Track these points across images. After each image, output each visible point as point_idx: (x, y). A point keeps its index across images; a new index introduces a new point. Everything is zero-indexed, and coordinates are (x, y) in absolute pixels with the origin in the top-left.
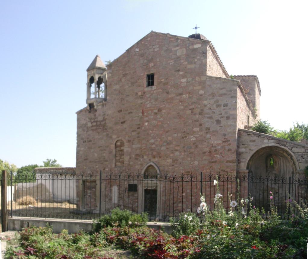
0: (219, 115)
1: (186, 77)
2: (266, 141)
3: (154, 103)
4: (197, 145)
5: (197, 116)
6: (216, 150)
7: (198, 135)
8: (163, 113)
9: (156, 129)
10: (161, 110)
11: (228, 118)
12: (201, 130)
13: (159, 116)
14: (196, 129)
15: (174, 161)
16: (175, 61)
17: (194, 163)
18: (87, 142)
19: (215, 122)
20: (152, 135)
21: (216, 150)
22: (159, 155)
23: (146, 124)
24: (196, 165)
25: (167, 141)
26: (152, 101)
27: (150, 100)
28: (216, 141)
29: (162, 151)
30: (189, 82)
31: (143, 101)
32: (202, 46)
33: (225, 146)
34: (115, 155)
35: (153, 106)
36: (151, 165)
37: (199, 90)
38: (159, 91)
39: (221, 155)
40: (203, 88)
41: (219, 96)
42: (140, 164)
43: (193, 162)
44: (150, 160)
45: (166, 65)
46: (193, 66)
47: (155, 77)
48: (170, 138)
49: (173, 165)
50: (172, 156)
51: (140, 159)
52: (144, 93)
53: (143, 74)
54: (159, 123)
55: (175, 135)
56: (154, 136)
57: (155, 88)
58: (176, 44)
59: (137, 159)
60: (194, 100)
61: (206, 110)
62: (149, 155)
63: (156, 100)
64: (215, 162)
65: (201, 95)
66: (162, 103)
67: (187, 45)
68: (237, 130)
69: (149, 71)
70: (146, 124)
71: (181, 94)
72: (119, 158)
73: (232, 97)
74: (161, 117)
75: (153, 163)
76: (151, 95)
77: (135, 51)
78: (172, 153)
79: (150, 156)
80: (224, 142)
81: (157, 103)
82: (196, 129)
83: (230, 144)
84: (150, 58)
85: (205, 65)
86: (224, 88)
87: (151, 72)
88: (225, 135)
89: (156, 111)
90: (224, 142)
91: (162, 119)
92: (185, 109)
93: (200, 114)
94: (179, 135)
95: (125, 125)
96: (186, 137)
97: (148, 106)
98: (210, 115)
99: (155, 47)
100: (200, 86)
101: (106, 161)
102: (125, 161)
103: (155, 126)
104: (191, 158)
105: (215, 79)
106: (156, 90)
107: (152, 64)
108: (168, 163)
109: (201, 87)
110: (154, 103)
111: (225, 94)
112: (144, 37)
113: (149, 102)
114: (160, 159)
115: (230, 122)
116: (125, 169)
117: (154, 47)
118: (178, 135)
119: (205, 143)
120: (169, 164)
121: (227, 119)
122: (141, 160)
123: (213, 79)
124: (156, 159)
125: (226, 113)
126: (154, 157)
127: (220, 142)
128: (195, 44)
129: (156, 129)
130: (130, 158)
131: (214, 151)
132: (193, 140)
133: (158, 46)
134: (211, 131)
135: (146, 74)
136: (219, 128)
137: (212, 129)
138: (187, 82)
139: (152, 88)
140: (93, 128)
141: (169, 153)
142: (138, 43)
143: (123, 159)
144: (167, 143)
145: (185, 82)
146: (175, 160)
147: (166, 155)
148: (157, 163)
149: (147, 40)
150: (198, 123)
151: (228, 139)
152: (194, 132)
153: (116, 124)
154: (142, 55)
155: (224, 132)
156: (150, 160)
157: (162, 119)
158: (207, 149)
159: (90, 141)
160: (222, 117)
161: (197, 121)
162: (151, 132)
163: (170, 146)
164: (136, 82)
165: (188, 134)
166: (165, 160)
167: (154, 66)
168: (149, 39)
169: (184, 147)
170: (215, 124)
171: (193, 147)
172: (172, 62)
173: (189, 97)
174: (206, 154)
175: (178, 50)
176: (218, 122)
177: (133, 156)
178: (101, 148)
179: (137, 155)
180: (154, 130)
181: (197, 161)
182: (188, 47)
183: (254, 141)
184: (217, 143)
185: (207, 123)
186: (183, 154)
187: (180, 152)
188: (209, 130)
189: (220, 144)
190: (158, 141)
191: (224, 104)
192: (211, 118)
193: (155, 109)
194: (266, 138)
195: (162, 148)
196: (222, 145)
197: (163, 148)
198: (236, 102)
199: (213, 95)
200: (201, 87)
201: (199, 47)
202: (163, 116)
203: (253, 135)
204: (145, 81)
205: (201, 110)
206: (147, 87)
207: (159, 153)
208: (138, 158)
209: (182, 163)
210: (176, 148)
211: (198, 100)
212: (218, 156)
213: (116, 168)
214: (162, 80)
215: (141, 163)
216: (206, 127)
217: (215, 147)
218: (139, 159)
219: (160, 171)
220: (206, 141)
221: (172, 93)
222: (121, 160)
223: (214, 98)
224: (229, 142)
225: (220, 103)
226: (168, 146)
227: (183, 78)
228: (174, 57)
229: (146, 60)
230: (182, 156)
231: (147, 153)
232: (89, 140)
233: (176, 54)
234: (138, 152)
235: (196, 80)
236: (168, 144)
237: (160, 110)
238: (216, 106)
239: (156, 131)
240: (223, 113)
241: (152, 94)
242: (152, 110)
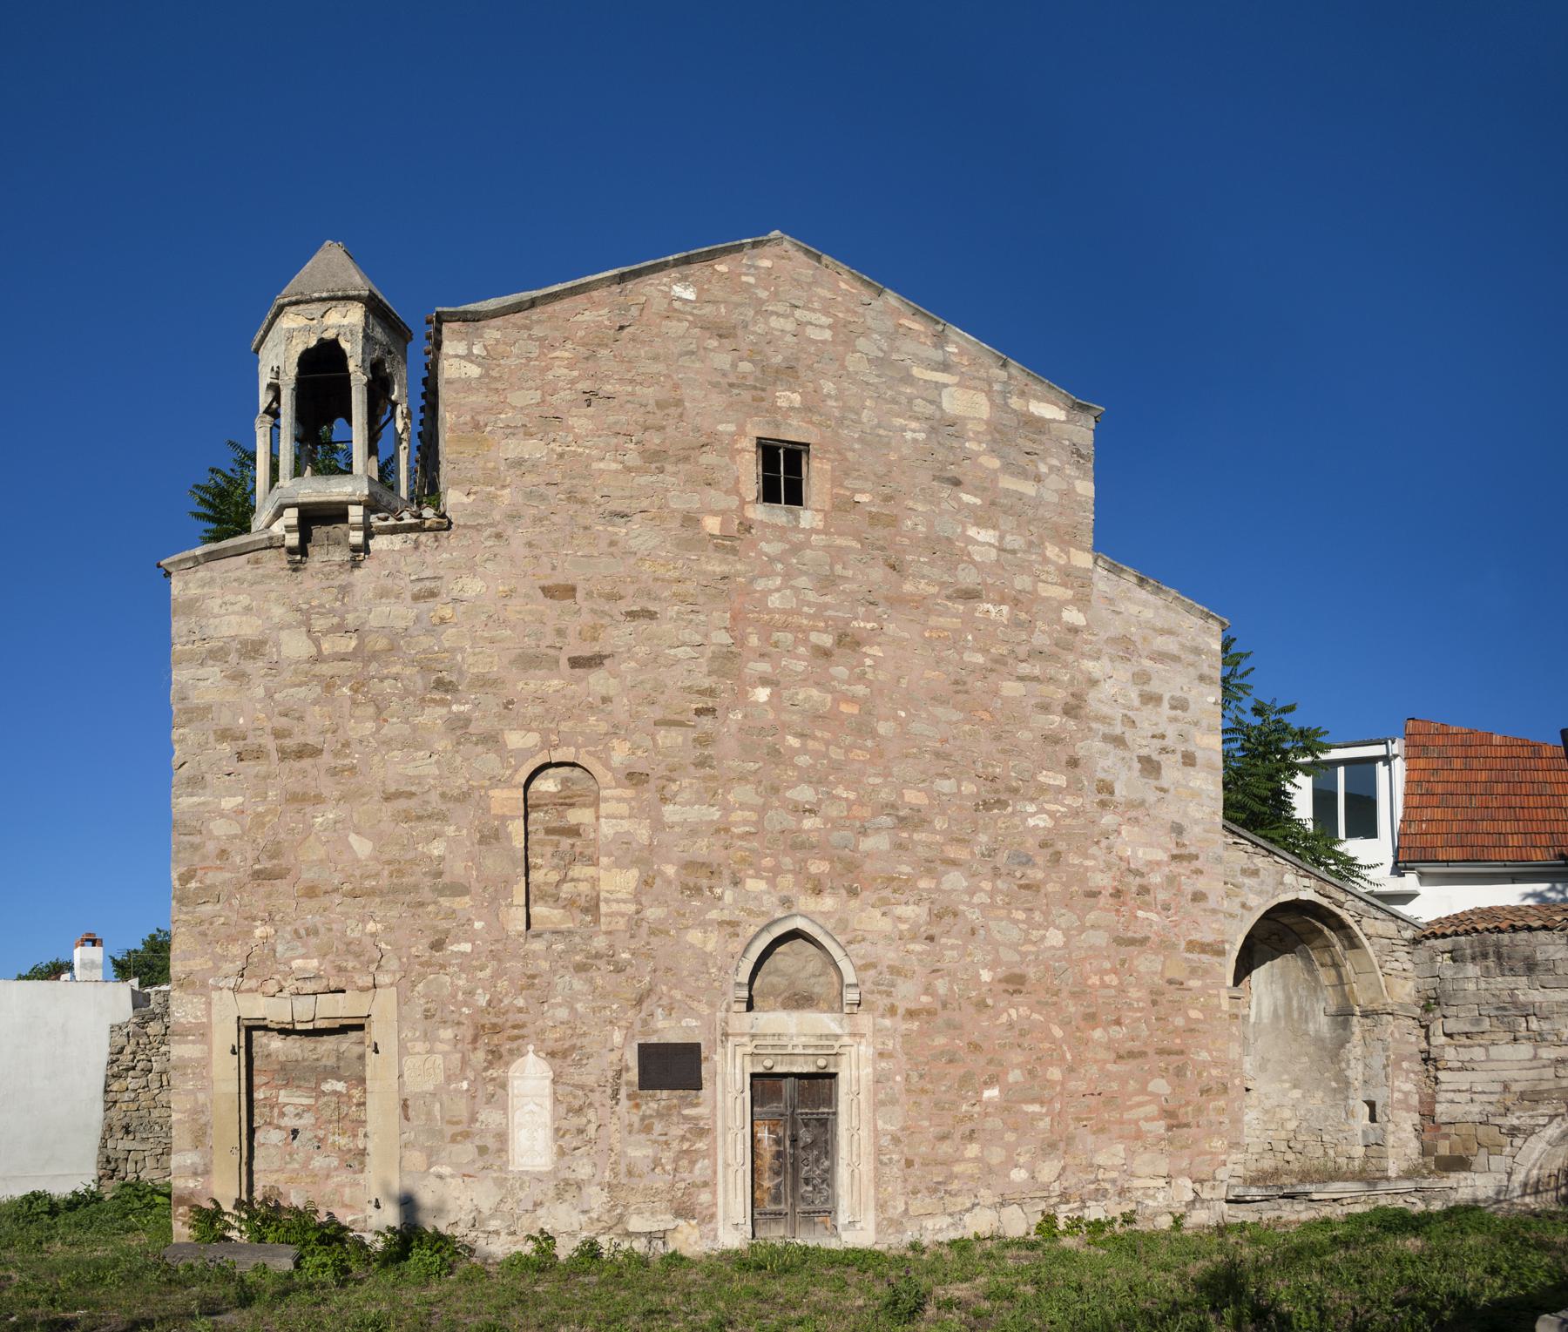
8: (868, 662)
9: (827, 735)
10: (858, 644)
13: (840, 671)
18: (275, 756)
20: (803, 760)
22: (850, 876)
25: (893, 806)
26: (802, 581)
27: (788, 576)
29: (868, 855)
31: (739, 567)
35: (805, 609)
36: (795, 934)
38: (840, 541)
42: (721, 923)
44: (786, 902)
48: (913, 797)
49: (931, 938)
50: (929, 890)
51: (718, 891)
54: (844, 708)
56: (813, 766)
57: (821, 525)
59: (697, 890)
62: (777, 871)
63: (827, 582)
66: (861, 610)
69: (777, 426)
70: (762, 694)
74: (861, 678)
76: (784, 552)
78: (930, 872)
79: (787, 882)
81: (827, 599)
84: (778, 359)
87: (793, 432)
89: (827, 640)
91: (860, 690)
95: (598, 681)
99: (812, 317)
101: (459, 890)
102: (603, 895)
103: (818, 718)
106: (825, 531)
107: (788, 398)
110: (812, 596)
113: (778, 581)
114: (854, 903)
116: (611, 946)
117: (798, 313)
120: (904, 927)
122: (729, 896)
124: (828, 903)
126: (818, 891)
129: (827, 735)
130: (647, 883)
139: (797, 518)
140: (325, 669)
141: (906, 869)
143: (584, 887)
144: (901, 819)
146: (943, 913)
147: (892, 879)
148: (829, 927)
149: (757, 268)
153: (529, 661)
156: (786, 902)
157: (860, 690)
159: (303, 752)
162: (793, 742)
163: (916, 836)
166: (884, 901)
167: (807, 409)
168: (766, 263)
177: (670, 870)
178: (402, 804)
179: (690, 866)
180: (814, 738)
190: (840, 798)
193: (814, 629)
195: (867, 844)
202: (870, 676)
207: (851, 866)
208: (704, 882)
209: (982, 932)
210: (952, 852)
213: (538, 935)
215: (726, 915)
218: (711, 889)
219: (859, 969)
222: (567, 888)
226: (905, 835)
230: (981, 898)
231: (767, 862)
232: (289, 743)
236: (902, 821)
237: (849, 641)
239: (827, 743)
241: (796, 549)
242: (806, 631)
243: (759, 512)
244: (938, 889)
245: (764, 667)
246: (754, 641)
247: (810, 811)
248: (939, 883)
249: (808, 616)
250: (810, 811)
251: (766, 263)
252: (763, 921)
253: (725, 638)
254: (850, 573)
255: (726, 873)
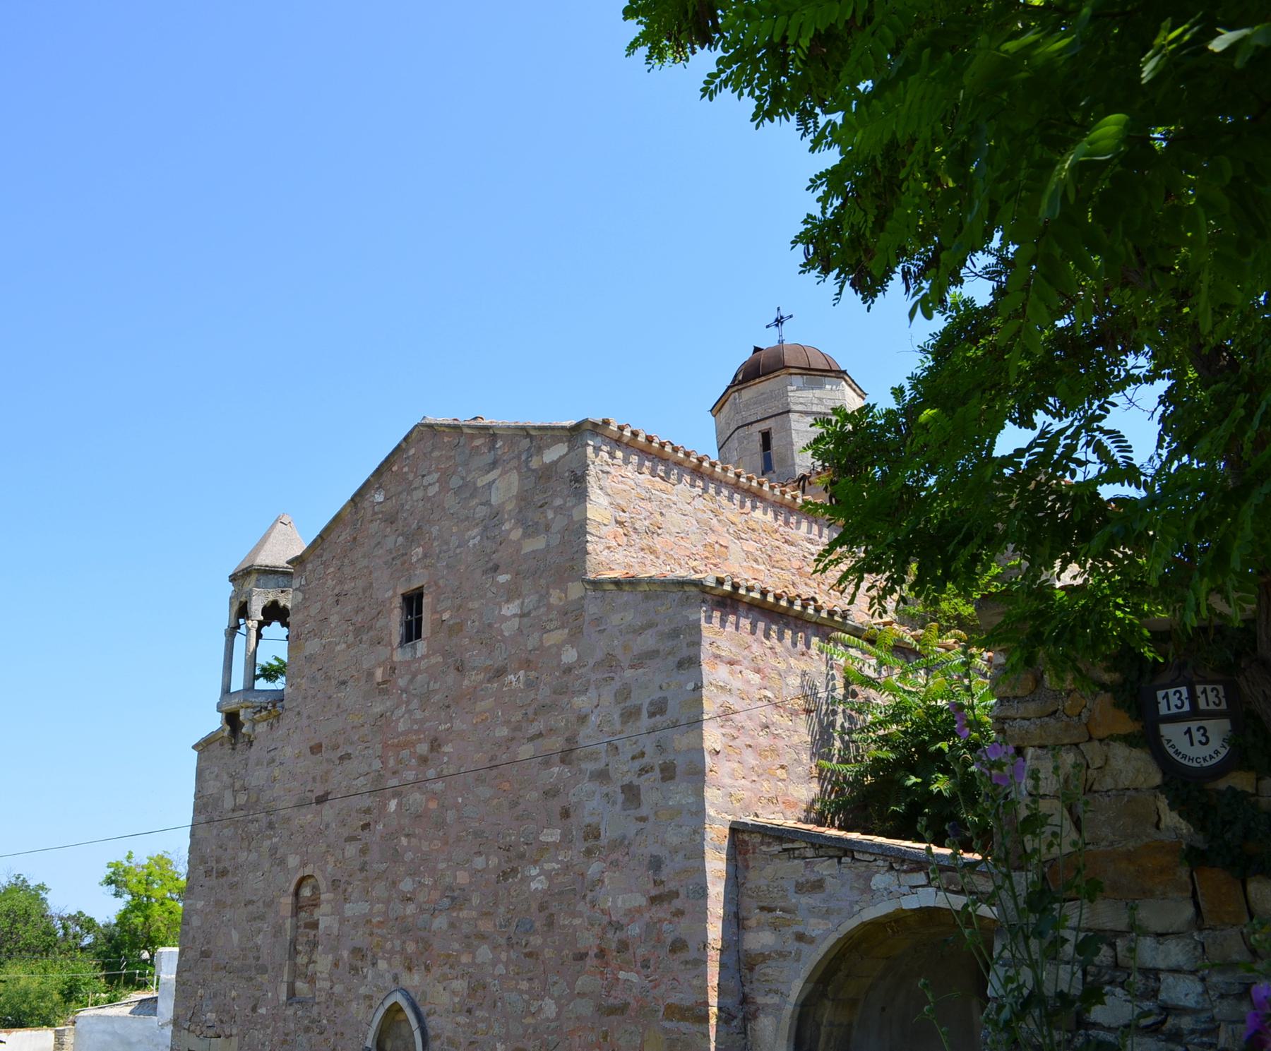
0: (633, 758)
1: (519, 596)
2: (881, 880)
3: (418, 715)
4: (552, 915)
5: (556, 770)
6: (623, 946)
7: (558, 862)
11: (668, 773)
12: (566, 840)
14: (551, 836)
15: (473, 991)
16: (486, 528)
17: (540, 1009)
19: (620, 798)
21: (623, 946)
23: (393, 805)
24: (548, 1019)
28: (622, 896)
30: (529, 613)
31: (388, 704)
32: (571, 449)
33: (660, 921)
34: (293, 943)
37: (559, 647)
39: (644, 972)
40: (575, 636)
41: (632, 667)
43: (536, 1004)
44: (396, 978)
45: (458, 551)
46: (538, 543)
47: (425, 601)
48: (462, 878)
49: (469, 1011)
52: (393, 669)
53: (390, 593)
55: (479, 862)
58: (489, 458)
59: (355, 970)
60: (544, 693)
61: (586, 736)
63: (425, 698)
64: (621, 1009)
65: (568, 670)
67: (523, 458)
68: (716, 834)
69: (409, 580)
71: (500, 673)
72: (305, 960)
73: (680, 665)
75: (405, 993)
77: (373, 505)
80: (654, 900)
82: (551, 836)
83: (679, 913)
85: (579, 530)
86: (651, 625)
88: (656, 864)
90: (654, 900)
92: (513, 739)
93: (563, 761)
94: (494, 861)
96: (514, 871)
97: (401, 727)
98: (600, 765)
99: (429, 479)
100: (562, 627)
104: (530, 979)
105: (612, 587)
108: (454, 993)
109: (566, 631)
111: (653, 654)
112: (398, 448)
115: (678, 794)
118: (487, 860)
119: (581, 906)
121: (664, 779)
123: (607, 587)
125: (660, 748)
127: (641, 901)
128: (548, 447)
131: (614, 946)
132: (540, 887)
133: (436, 476)
134: (604, 841)
135: (401, 591)
136: (633, 828)
137: (607, 835)
138: (522, 616)
142: (379, 472)
144: (453, 899)
145: (515, 616)
146: (477, 987)
150: (556, 805)
151: (672, 885)
152: (544, 848)
154: (391, 520)
155: (655, 850)
156: (396, 978)
158: (589, 941)
160: (644, 771)
161: (551, 793)
162: (404, 841)
164: (370, 628)
165: (522, 856)
166: (445, 977)
167: (425, 556)
169: (508, 923)
170: (618, 807)
171: (537, 924)
172: (474, 537)
173: (530, 684)
174: (591, 962)
175: (494, 481)
176: (632, 793)
177: (345, 954)
179: (357, 952)
181: (551, 997)
182: (527, 461)
183: (818, 885)
184: (628, 905)
185: (594, 804)
186: (504, 956)
187: (495, 948)
188: (597, 837)
189: (639, 910)
191: (651, 704)
192: (602, 776)
194: (880, 863)
196: (647, 916)
197: (440, 922)
198: (698, 687)
199: (609, 663)
200: (566, 631)
201: (561, 458)
203: (810, 853)
204: (395, 622)
205: (567, 740)
206: (401, 645)
211: (555, 692)
212: (633, 977)
214: (446, 616)
216: (588, 820)
217: (618, 927)
220: (584, 897)
221: (474, 669)
223: (613, 679)
224: (677, 903)
225: (634, 700)
227: (508, 601)
228: (481, 512)
229: (402, 534)
230: (500, 970)
231: (388, 945)
233: (487, 503)
234: (360, 938)
235: (552, 600)
237: (435, 745)
238: (622, 715)
240: (650, 749)
243: (398, 656)
244: (474, 963)
245: (394, 782)
246: (391, 763)
247: (410, 899)
248: (474, 958)
249: (417, 732)
250: (410, 899)
251: (412, 452)
252: (385, 993)
253: (377, 764)
254: (437, 686)
255: (369, 954)
